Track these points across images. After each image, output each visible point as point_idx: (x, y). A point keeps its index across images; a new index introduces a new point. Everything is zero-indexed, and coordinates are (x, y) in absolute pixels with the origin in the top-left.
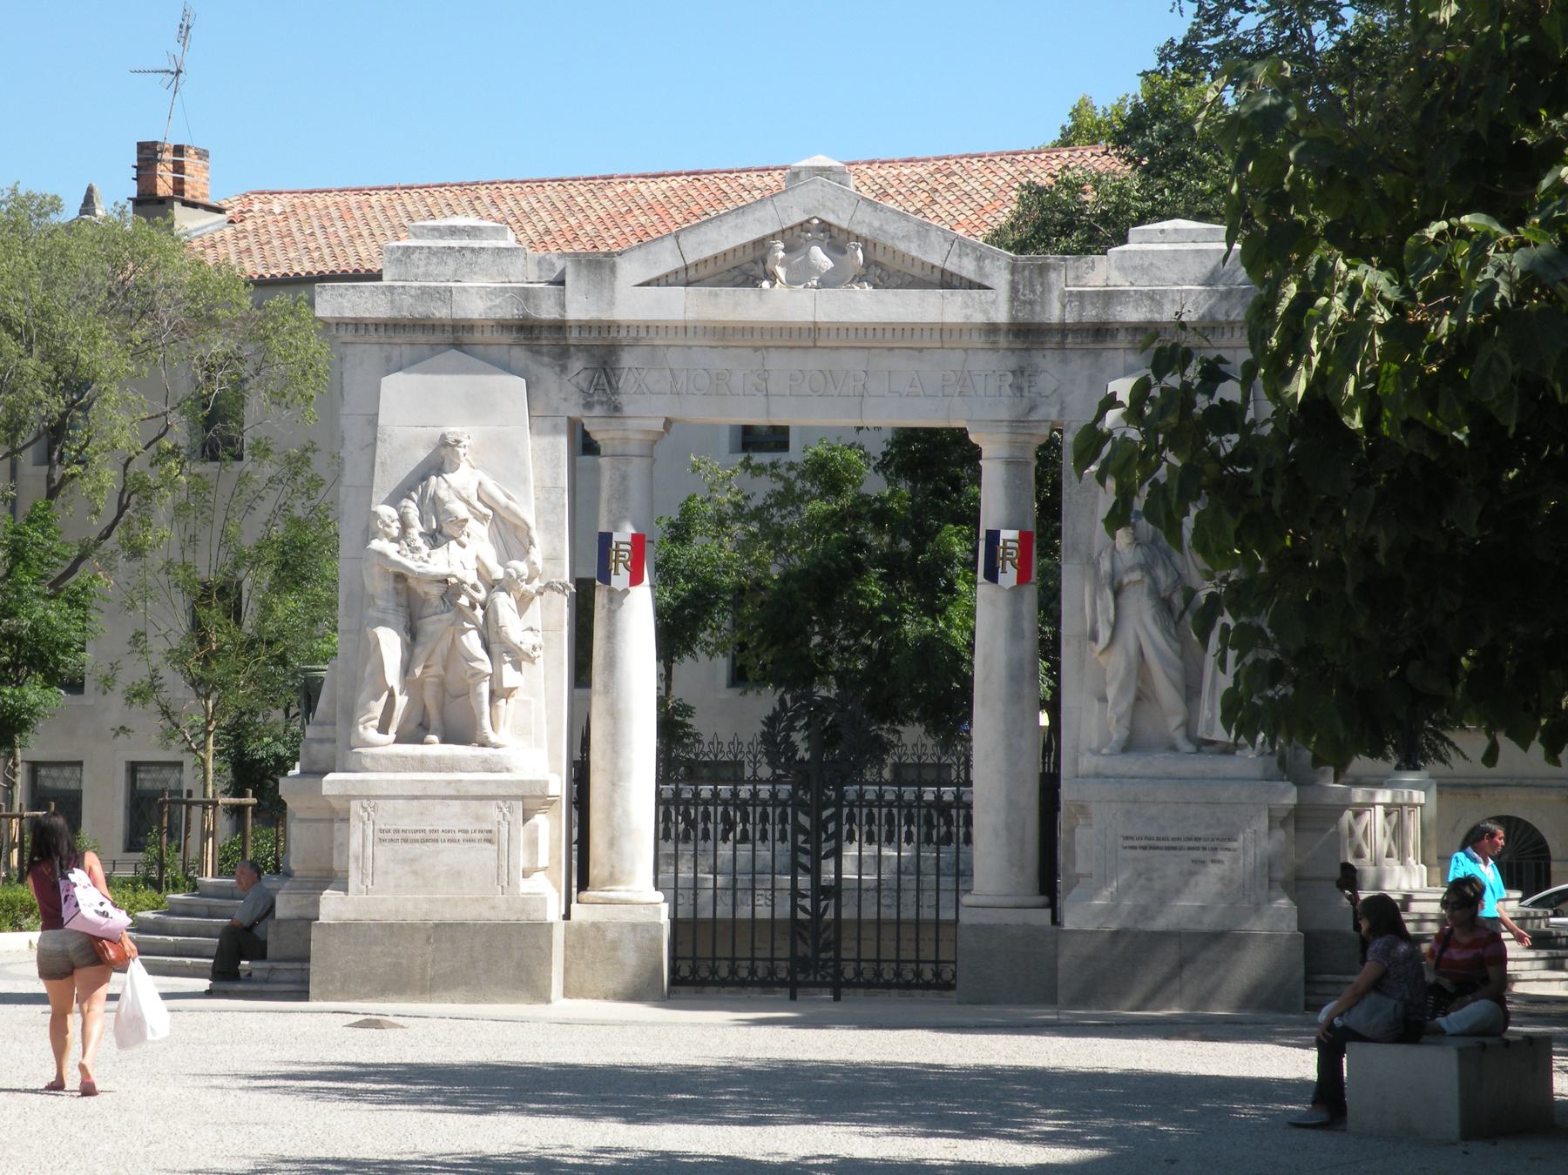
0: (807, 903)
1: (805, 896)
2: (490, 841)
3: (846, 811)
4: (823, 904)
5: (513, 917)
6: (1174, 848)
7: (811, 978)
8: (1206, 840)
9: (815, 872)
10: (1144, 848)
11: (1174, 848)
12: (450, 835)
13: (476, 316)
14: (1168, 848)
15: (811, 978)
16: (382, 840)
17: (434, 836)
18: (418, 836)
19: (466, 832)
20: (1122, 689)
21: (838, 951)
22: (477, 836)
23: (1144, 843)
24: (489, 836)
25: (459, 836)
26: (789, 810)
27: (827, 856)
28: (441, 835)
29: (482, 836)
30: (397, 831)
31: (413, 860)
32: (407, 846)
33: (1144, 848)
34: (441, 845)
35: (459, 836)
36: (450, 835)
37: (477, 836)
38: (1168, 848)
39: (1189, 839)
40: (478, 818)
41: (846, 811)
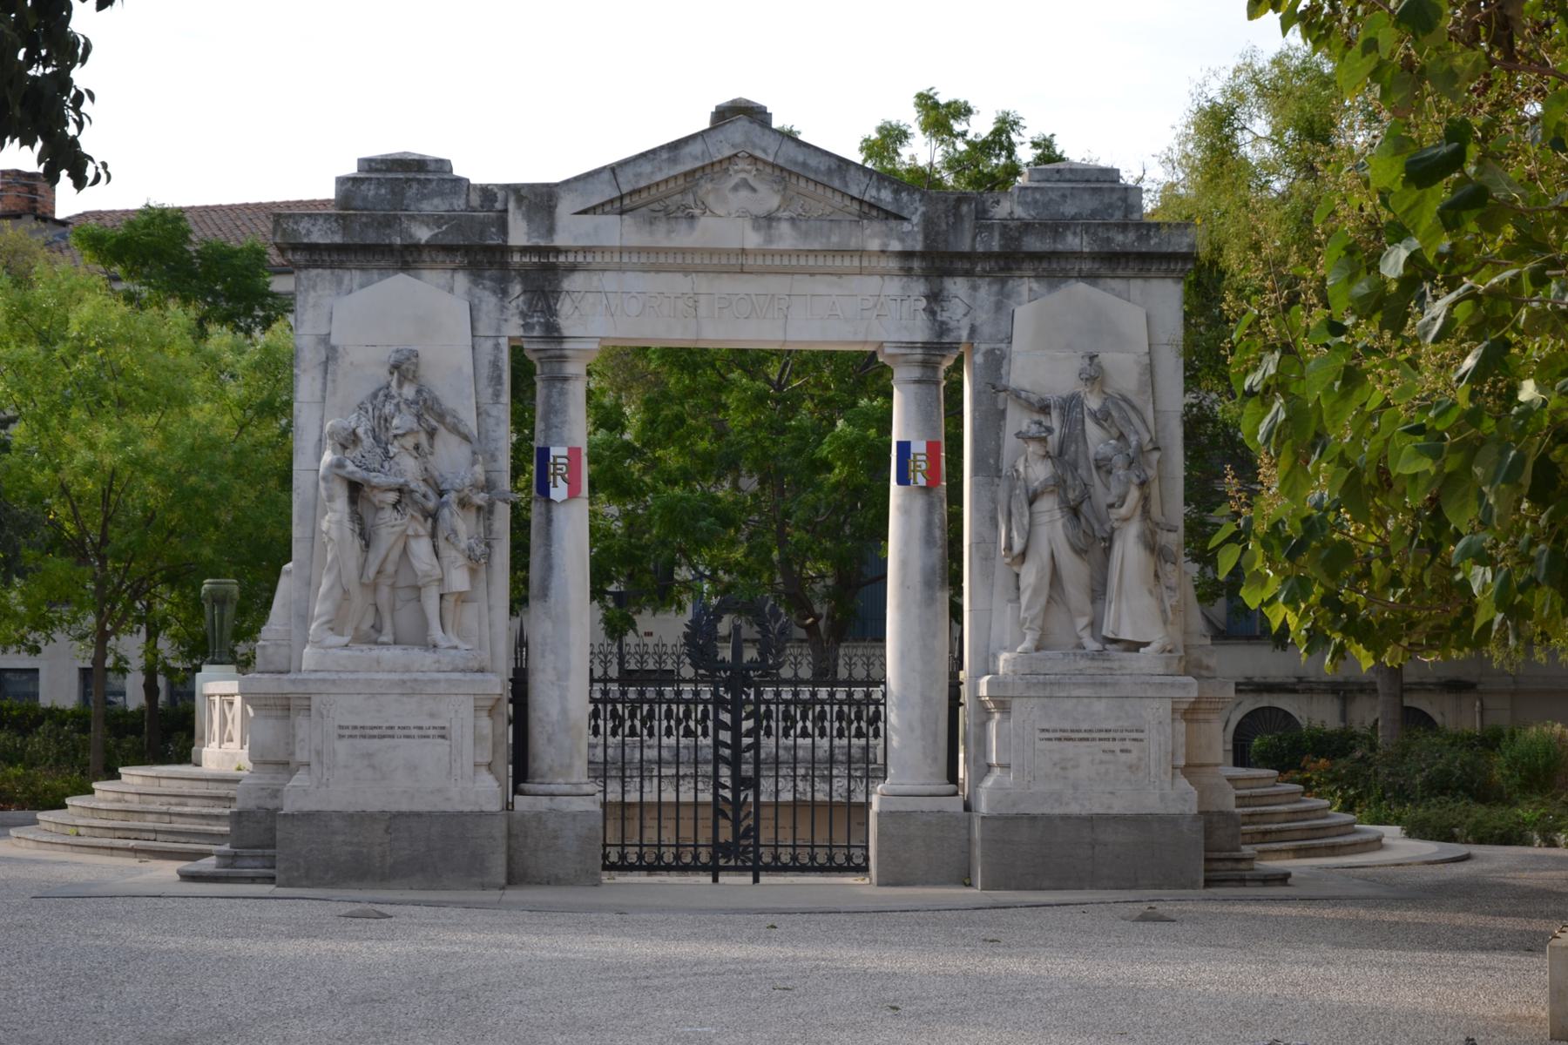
2: (443, 737)
12: (406, 732)
16: (341, 737)
17: (390, 732)
18: (375, 732)
19: (421, 728)
25: (415, 732)
30: (355, 728)
31: (369, 755)
36: (406, 732)
40: (432, 715)
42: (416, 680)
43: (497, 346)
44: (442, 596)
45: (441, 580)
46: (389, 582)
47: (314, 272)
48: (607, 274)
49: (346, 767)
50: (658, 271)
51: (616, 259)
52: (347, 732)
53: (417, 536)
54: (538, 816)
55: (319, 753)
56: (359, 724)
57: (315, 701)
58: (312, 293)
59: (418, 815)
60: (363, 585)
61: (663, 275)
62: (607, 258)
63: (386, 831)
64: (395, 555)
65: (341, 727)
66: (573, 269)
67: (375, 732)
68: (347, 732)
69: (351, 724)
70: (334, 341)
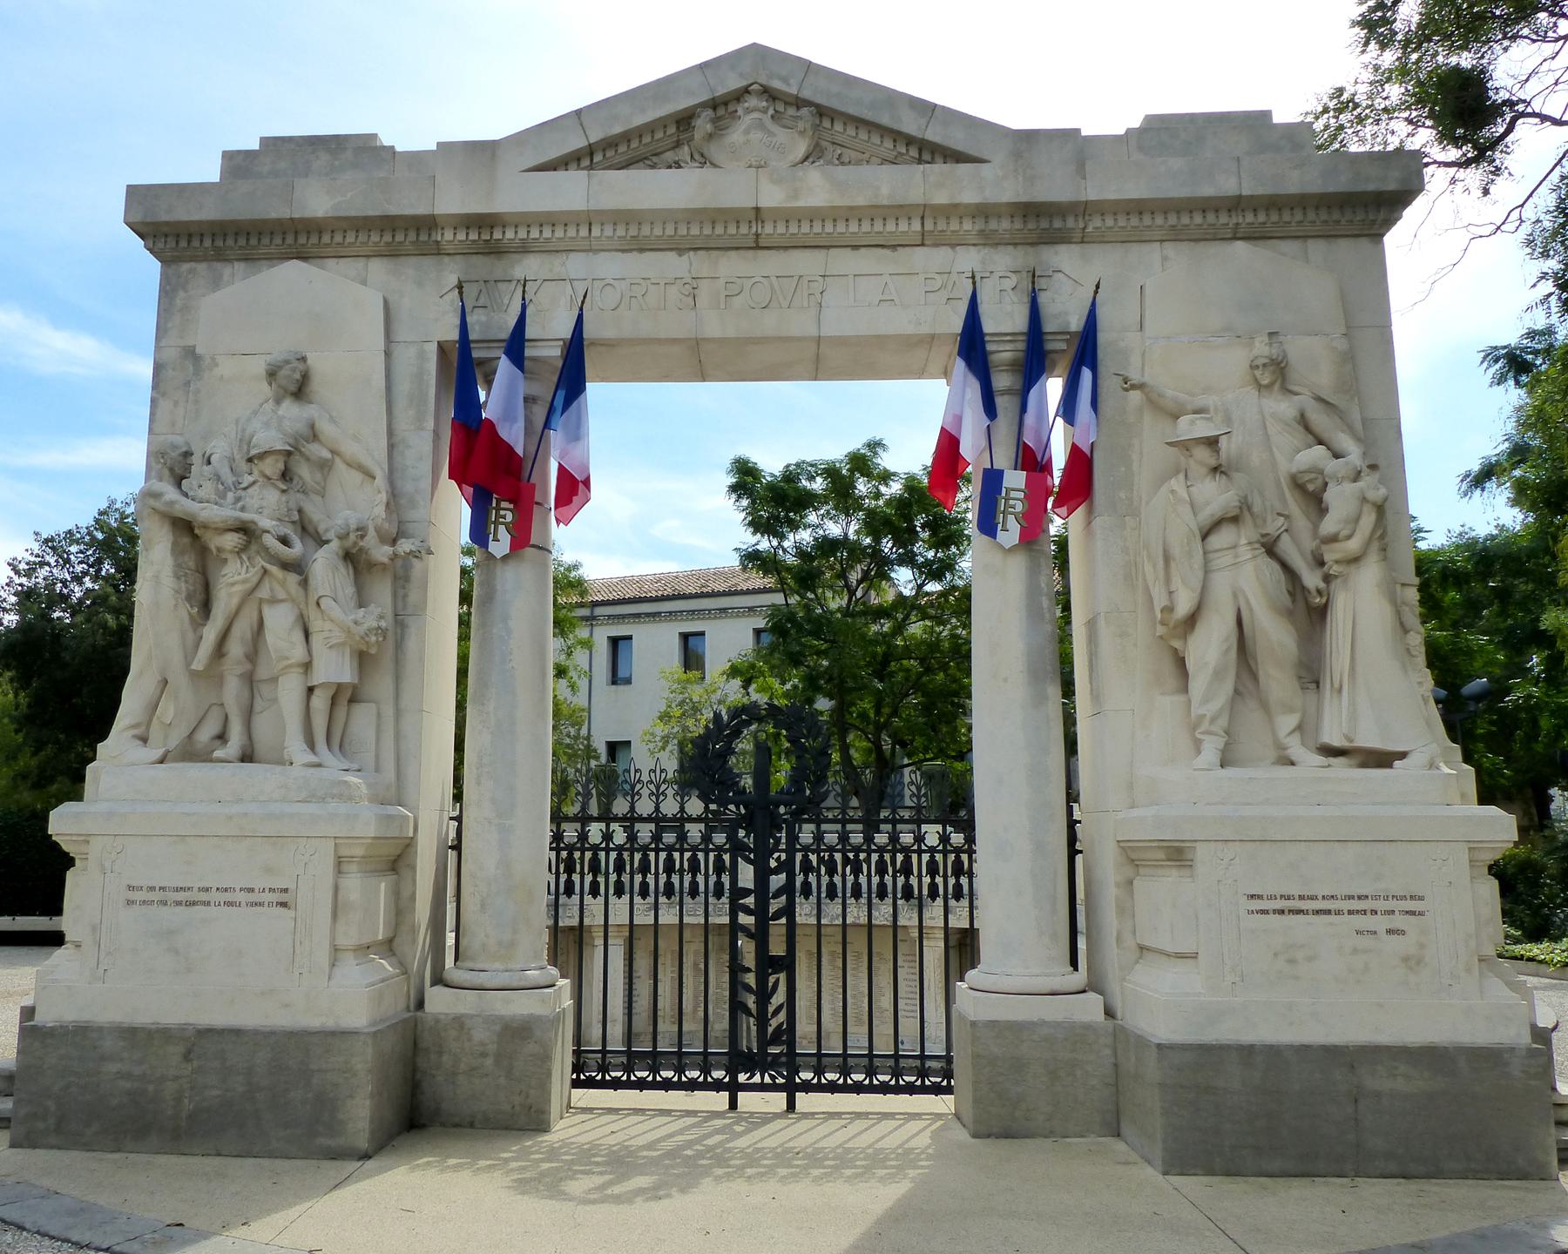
0: (751, 979)
1: (749, 970)
2: (284, 905)
3: (799, 856)
4: (772, 980)
5: (314, 1022)
6: (1328, 912)
7: (757, 1079)
8: (1376, 898)
9: (760, 936)
10: (1282, 912)
11: (1328, 912)
12: (228, 897)
13: (320, 214)
14: (1318, 912)
15: (757, 1079)
16: (130, 902)
17: (203, 896)
18: (181, 896)
19: (251, 890)
20: (1218, 675)
21: (791, 1044)
23: (1279, 904)
24: (283, 897)
25: (242, 897)
26: (727, 857)
27: (777, 916)
28: (214, 896)
29: (275, 897)
30: (152, 889)
33: (1282, 912)
34: (212, 910)
35: (242, 897)
36: (228, 897)
37: (268, 897)
38: (1318, 912)
39: (1351, 897)
40: (268, 870)
41: (799, 856)
43: (422, 355)
44: (311, 690)
45: (307, 666)
46: (239, 670)
47: (185, 267)
48: (572, 255)
50: (641, 250)
51: (584, 232)
52: (138, 896)
53: (274, 601)
54: (459, 1022)
55: (94, 929)
58: (181, 294)
59: (237, 1032)
60: (194, 675)
61: (648, 254)
62: (572, 232)
63: (187, 1057)
64: (242, 629)
65: (131, 888)
66: (525, 249)
67: (181, 896)
68: (138, 896)
69: (145, 883)
70: (199, 350)
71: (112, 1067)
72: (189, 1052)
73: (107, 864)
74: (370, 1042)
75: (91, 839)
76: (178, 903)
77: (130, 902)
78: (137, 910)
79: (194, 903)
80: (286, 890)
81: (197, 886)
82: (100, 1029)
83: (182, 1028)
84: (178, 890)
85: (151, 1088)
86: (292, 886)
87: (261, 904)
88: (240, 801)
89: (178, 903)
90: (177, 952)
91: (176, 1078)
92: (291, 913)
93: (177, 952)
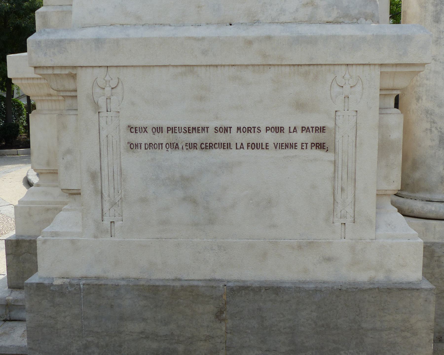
2: (320, 146)
5: (362, 276)
12: (252, 137)
16: (134, 146)
17: (222, 138)
18: (195, 138)
19: (279, 130)
22: (300, 137)
24: (320, 137)
25: (269, 138)
30: (158, 130)
31: (185, 181)
32: (177, 156)
34: (233, 153)
36: (252, 137)
37: (300, 137)
40: (300, 106)
42: (269, 38)
49: (144, 200)
52: (142, 138)
55: (94, 176)
56: (165, 124)
57: (85, 80)
59: (274, 290)
63: (219, 315)
65: (132, 129)
67: (195, 138)
68: (142, 138)
69: (149, 123)
71: (135, 327)
72: (221, 312)
73: (102, 102)
74: (433, 298)
75: (81, 73)
76: (193, 146)
77: (134, 146)
78: (142, 152)
79: (210, 146)
80: (322, 129)
81: (212, 125)
82: (116, 287)
83: (212, 284)
84: (190, 130)
85: (181, 348)
86: (329, 124)
87: (293, 146)
88: (255, 22)
89: (193, 146)
90: (194, 202)
91: (208, 338)
92: (330, 156)
93: (194, 202)
